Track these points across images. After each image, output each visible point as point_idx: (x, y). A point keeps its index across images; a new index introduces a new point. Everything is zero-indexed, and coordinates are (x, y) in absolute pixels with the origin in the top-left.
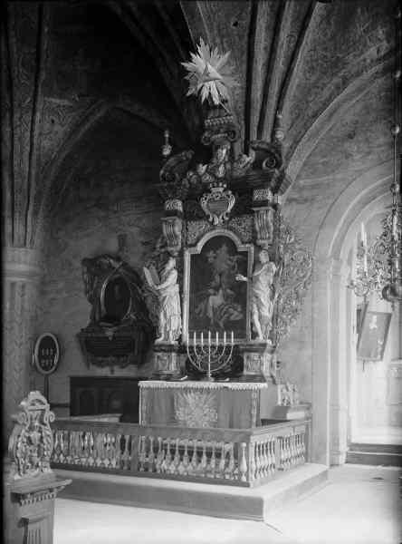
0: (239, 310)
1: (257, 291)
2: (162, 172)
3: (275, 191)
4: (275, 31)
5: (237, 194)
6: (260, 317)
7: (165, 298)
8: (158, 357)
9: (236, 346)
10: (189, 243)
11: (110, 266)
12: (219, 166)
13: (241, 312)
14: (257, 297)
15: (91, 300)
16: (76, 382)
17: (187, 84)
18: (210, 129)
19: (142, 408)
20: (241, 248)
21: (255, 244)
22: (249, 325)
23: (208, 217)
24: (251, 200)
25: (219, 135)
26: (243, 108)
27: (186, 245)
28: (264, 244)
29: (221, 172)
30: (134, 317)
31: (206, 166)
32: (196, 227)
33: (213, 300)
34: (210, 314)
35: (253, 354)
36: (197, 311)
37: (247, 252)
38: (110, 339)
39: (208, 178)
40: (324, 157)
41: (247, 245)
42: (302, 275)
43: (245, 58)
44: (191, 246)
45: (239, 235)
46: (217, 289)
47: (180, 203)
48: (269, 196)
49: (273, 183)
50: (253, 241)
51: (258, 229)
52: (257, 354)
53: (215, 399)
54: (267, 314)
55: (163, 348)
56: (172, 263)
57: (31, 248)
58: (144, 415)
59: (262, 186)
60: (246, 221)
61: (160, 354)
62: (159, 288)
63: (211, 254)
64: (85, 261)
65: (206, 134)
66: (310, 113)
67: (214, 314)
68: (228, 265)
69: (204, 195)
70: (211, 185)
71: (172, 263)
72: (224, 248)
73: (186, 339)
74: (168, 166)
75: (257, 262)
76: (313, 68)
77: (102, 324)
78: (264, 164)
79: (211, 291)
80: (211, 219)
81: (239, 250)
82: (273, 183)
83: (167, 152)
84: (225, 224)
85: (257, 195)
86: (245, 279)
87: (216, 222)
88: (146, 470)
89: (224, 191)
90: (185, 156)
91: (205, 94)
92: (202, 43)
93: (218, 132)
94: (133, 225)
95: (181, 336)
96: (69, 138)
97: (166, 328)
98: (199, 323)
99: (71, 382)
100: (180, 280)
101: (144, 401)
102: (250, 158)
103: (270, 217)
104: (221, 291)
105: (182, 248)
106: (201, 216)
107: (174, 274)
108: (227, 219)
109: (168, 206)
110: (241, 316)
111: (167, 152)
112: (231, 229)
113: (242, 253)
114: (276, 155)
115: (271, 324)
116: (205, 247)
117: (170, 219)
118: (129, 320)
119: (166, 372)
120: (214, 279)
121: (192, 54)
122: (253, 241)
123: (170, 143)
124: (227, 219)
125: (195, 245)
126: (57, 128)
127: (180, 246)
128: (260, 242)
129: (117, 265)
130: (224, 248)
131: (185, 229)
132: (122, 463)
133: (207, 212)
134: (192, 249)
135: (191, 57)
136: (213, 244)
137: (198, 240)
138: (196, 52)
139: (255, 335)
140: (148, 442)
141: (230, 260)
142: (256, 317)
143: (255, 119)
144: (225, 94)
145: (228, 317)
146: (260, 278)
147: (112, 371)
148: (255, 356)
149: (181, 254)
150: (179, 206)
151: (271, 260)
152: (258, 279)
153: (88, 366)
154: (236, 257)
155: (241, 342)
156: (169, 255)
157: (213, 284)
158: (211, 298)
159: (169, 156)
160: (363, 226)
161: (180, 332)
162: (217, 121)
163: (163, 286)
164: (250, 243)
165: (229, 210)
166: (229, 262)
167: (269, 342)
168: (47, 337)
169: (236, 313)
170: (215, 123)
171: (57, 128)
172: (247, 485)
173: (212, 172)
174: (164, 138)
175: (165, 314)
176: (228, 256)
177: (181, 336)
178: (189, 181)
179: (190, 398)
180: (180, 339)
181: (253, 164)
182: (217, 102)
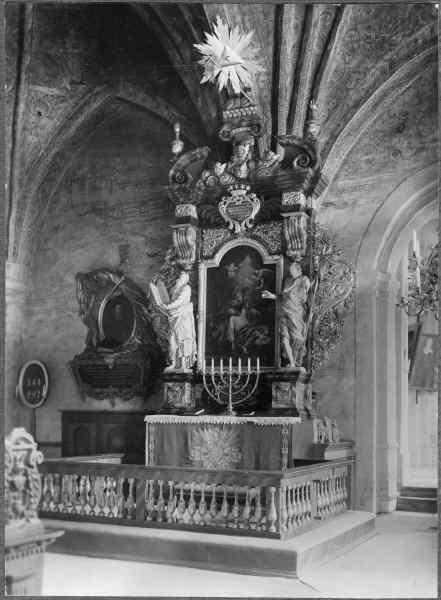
1: (287, 311)
2: (172, 172)
3: (309, 193)
5: (262, 197)
6: (292, 341)
7: (176, 319)
8: (169, 388)
9: (261, 375)
10: (205, 254)
11: (110, 283)
12: (240, 165)
13: (268, 335)
14: (287, 317)
15: (86, 322)
16: (69, 417)
17: (201, 70)
18: (230, 121)
20: (268, 260)
21: (285, 256)
22: (277, 350)
23: (228, 224)
24: (281, 203)
25: (241, 129)
26: (269, 98)
27: (201, 257)
28: (296, 256)
29: (243, 172)
30: (139, 342)
31: (224, 165)
32: (213, 236)
33: (234, 321)
34: (232, 338)
35: (283, 383)
37: (275, 265)
38: (111, 367)
39: (228, 179)
40: (367, 154)
41: (276, 257)
42: (341, 292)
43: (271, 39)
44: (207, 258)
45: (266, 245)
46: (239, 308)
47: (193, 208)
48: (302, 199)
49: (306, 185)
50: (283, 251)
51: (287, 237)
52: (288, 384)
53: (238, 436)
54: (300, 336)
55: (175, 377)
56: (185, 278)
57: (14, 262)
59: (293, 188)
60: (274, 230)
61: (170, 384)
62: (169, 307)
63: (232, 267)
64: (79, 276)
65: (225, 128)
66: (351, 103)
68: (253, 280)
69: (223, 199)
70: (231, 188)
71: (185, 278)
72: (248, 260)
73: (202, 366)
74: (179, 165)
75: (288, 275)
76: (353, 50)
77: (100, 349)
78: (295, 163)
79: (232, 311)
80: (231, 227)
82: (306, 185)
83: (178, 147)
84: (249, 233)
85: (287, 199)
86: (273, 296)
87: (238, 229)
88: (155, 519)
89: (248, 193)
90: (200, 153)
91: (223, 82)
92: (219, 21)
93: (239, 126)
94: (137, 234)
95: (196, 362)
96: (59, 134)
98: (217, 347)
99: (63, 420)
100: (195, 298)
101: (152, 438)
102: (280, 155)
103: (303, 224)
104: (244, 311)
105: (197, 259)
106: (220, 224)
107: (187, 292)
108: (250, 226)
109: (180, 211)
110: (269, 340)
111: (178, 147)
112: (255, 238)
114: (310, 152)
115: (304, 348)
116: (226, 259)
117: (182, 227)
118: (133, 345)
119: (178, 405)
121: (207, 35)
122: (283, 251)
123: (182, 138)
124: (250, 226)
125: (212, 257)
126: (44, 121)
127: (193, 259)
128: (291, 253)
129: (118, 281)
130: (248, 260)
131: (200, 237)
132: (125, 511)
133: (227, 219)
134: (209, 261)
135: (205, 37)
137: (216, 251)
138: (211, 32)
139: (286, 361)
140: (156, 486)
141: (255, 274)
142: (286, 342)
143: (284, 111)
144: (249, 82)
145: (253, 342)
146: (292, 295)
147: (113, 405)
148: (286, 386)
149: (196, 267)
150: (193, 211)
151: (305, 272)
152: (288, 297)
153: (83, 399)
154: (261, 271)
155: (270, 369)
156: (181, 268)
158: (232, 318)
159: (180, 154)
160: (415, 234)
161: (195, 359)
162: (237, 113)
163: (174, 305)
164: (279, 254)
165: (253, 216)
166: (254, 277)
167: (303, 370)
168: (35, 365)
169: (262, 336)
170: (235, 115)
171: (44, 121)
172: (277, 536)
173: (232, 173)
174: (174, 133)
175: (177, 339)
176: (252, 269)
177: (196, 362)
178: (204, 182)
179: (208, 435)
180: (195, 367)
181: (282, 162)
182: (237, 90)
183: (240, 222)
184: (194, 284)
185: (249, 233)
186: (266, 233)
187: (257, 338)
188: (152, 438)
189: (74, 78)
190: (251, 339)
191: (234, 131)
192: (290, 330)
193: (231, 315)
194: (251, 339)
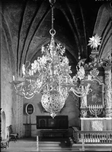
0: (101, 99)
4: (107, 33)
14: (108, 96)
19: (82, 125)
25: (94, 56)
34: (93, 100)
39: (91, 66)
41: (102, 83)
45: (100, 81)
53: (103, 122)
57: (20, 77)
58: (83, 127)
65: (91, 55)
67: (94, 100)
73: (86, 106)
79: (93, 94)
81: (100, 84)
83: (79, 58)
84: (96, 78)
88: (109, 142)
93: (94, 55)
96: (37, 47)
97: (83, 104)
104: (95, 94)
111: (79, 58)
112: (97, 79)
113: (100, 85)
123: (80, 55)
126: (35, 44)
132: (101, 141)
145: (98, 101)
146: (108, 92)
158: (93, 96)
162: (94, 53)
165: (97, 75)
169: (100, 100)
171: (35, 44)
173: (93, 65)
178: (86, 66)
179: (96, 122)
183: (94, 76)
185: (96, 78)
186: (99, 78)
187: (98, 100)
188: (82, 123)
189: (43, 35)
190: (97, 101)
191: (92, 56)
192: (108, 99)
193: (92, 95)
194: (97, 101)
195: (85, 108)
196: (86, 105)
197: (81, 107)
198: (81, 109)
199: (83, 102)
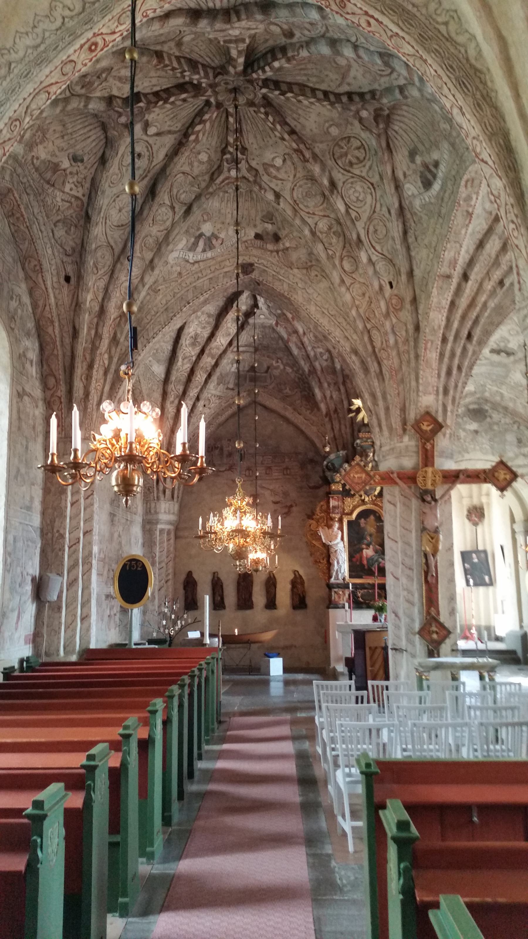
2: (325, 463)
27: (343, 513)
36: (354, 560)
44: (347, 514)
46: (368, 545)
61: (336, 590)
67: (368, 561)
72: (372, 517)
79: (364, 546)
84: (373, 503)
93: (366, 441)
100: (342, 539)
112: (376, 505)
116: (359, 516)
120: (366, 539)
130: (372, 517)
136: (364, 514)
157: (365, 541)
158: (364, 551)
163: (335, 542)
175: (338, 563)
180: (344, 579)
184: (341, 529)
195: (342, 581)
196: (347, 574)
197: (332, 580)
198: (332, 584)
199: (336, 567)
